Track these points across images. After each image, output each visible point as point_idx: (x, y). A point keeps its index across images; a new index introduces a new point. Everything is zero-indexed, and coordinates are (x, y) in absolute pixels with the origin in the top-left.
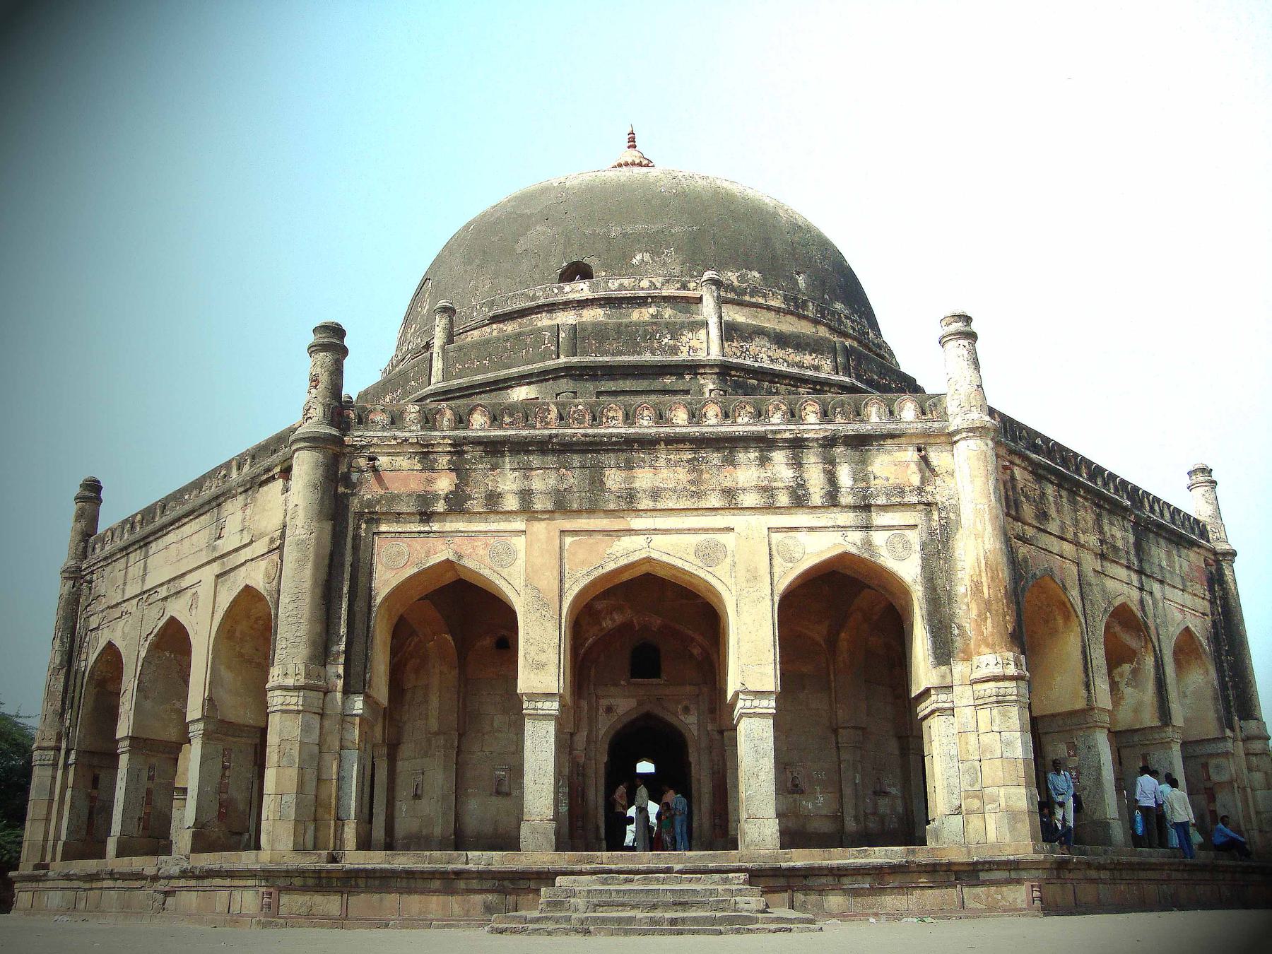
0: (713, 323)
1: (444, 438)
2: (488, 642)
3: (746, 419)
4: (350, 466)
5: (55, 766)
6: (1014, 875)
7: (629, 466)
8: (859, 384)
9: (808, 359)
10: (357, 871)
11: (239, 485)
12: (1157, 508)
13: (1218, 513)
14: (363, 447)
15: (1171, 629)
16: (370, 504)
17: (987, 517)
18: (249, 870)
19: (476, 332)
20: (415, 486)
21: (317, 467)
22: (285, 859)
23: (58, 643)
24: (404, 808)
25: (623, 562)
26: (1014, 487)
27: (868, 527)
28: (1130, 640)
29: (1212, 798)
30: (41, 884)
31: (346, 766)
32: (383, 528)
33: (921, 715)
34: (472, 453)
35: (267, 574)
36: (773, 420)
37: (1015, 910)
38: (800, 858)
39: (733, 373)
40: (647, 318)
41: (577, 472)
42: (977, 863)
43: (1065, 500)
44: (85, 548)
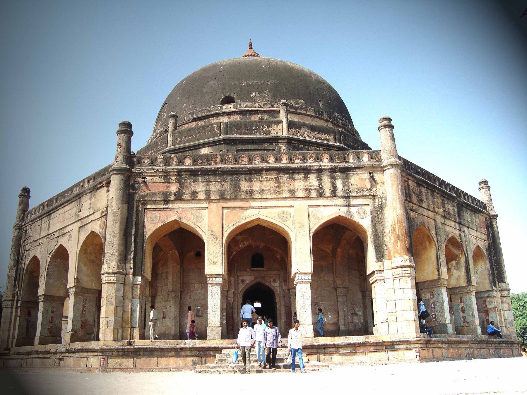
1: (173, 169)
2: (192, 253)
3: (299, 161)
4: (135, 181)
5: (12, 307)
6: (408, 346)
7: (251, 181)
8: (345, 147)
9: (324, 136)
10: (140, 348)
14: (140, 173)
15: (472, 246)
16: (143, 197)
17: (398, 201)
18: (94, 349)
19: (186, 126)
20: (162, 189)
21: (121, 182)
22: (110, 344)
23: (12, 256)
26: (409, 189)
27: (349, 205)
28: (455, 251)
29: (487, 314)
30: (7, 357)
31: (135, 306)
34: (185, 176)
35: (100, 226)
38: (322, 341)
39: (293, 142)
40: (257, 119)
41: (229, 182)
43: (429, 194)
44: (23, 216)
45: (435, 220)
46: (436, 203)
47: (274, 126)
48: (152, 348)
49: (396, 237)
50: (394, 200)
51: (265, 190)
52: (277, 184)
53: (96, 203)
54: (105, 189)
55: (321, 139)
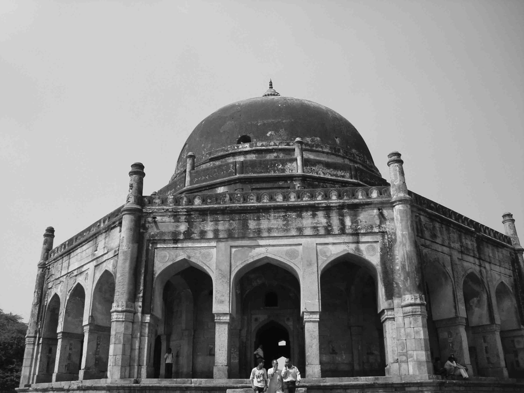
0: (299, 159)
1: (183, 209)
3: (307, 199)
4: (145, 221)
5: (34, 344)
6: (420, 389)
7: (258, 219)
8: (361, 183)
9: (339, 173)
11: (103, 229)
12: (487, 231)
13: (515, 233)
15: (494, 283)
16: (153, 236)
18: (102, 387)
19: (204, 166)
20: (171, 229)
21: (132, 221)
22: (117, 382)
23: (36, 294)
25: (256, 258)
26: (421, 224)
27: (358, 242)
28: (476, 288)
29: (517, 356)
32: (159, 246)
33: (382, 321)
34: (194, 215)
36: (318, 199)
39: (308, 179)
40: (273, 158)
41: (237, 221)
42: (404, 384)
43: (444, 229)
44: (47, 255)
45: (451, 256)
46: (452, 238)
47: (289, 165)
48: (158, 387)
49: (406, 275)
50: (403, 235)
51: (273, 228)
52: (285, 222)
53: (110, 242)
54: (118, 229)
55: (336, 176)
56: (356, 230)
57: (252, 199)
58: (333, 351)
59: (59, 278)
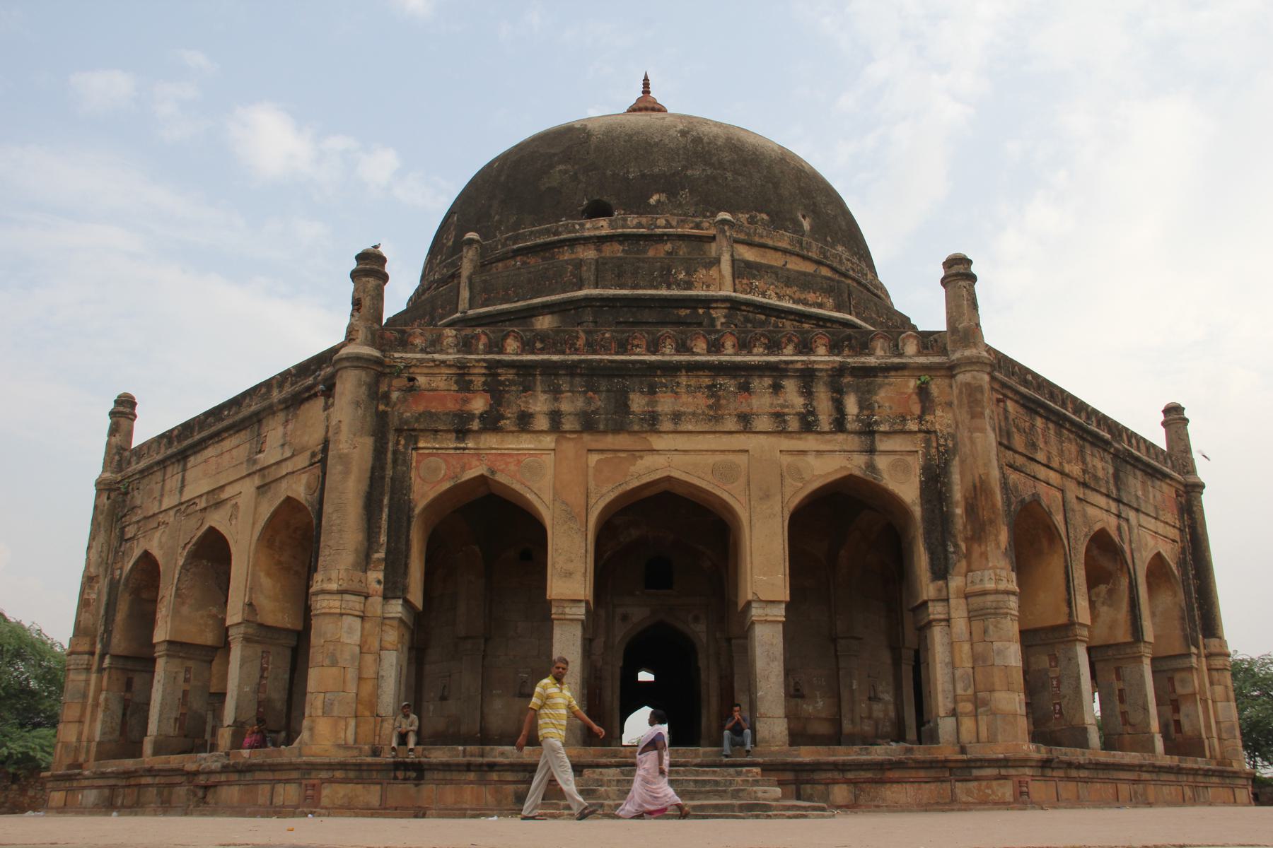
4: (390, 386)
6: (1003, 772)
7: (652, 391)
9: (811, 297)
11: (280, 402)
12: (1134, 441)
20: (451, 406)
24: (431, 708)
26: (1006, 418)
28: (1106, 563)
30: (75, 784)
34: (506, 375)
35: (308, 486)
37: (1004, 803)
41: (604, 395)
43: (1052, 432)
46: (1066, 453)
47: (702, 273)
51: (684, 413)
52: (711, 401)
53: (298, 433)
54: (320, 402)
56: (869, 425)
57: (637, 346)
58: (798, 690)
59: (154, 515)
